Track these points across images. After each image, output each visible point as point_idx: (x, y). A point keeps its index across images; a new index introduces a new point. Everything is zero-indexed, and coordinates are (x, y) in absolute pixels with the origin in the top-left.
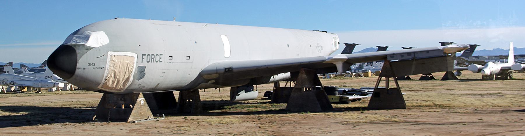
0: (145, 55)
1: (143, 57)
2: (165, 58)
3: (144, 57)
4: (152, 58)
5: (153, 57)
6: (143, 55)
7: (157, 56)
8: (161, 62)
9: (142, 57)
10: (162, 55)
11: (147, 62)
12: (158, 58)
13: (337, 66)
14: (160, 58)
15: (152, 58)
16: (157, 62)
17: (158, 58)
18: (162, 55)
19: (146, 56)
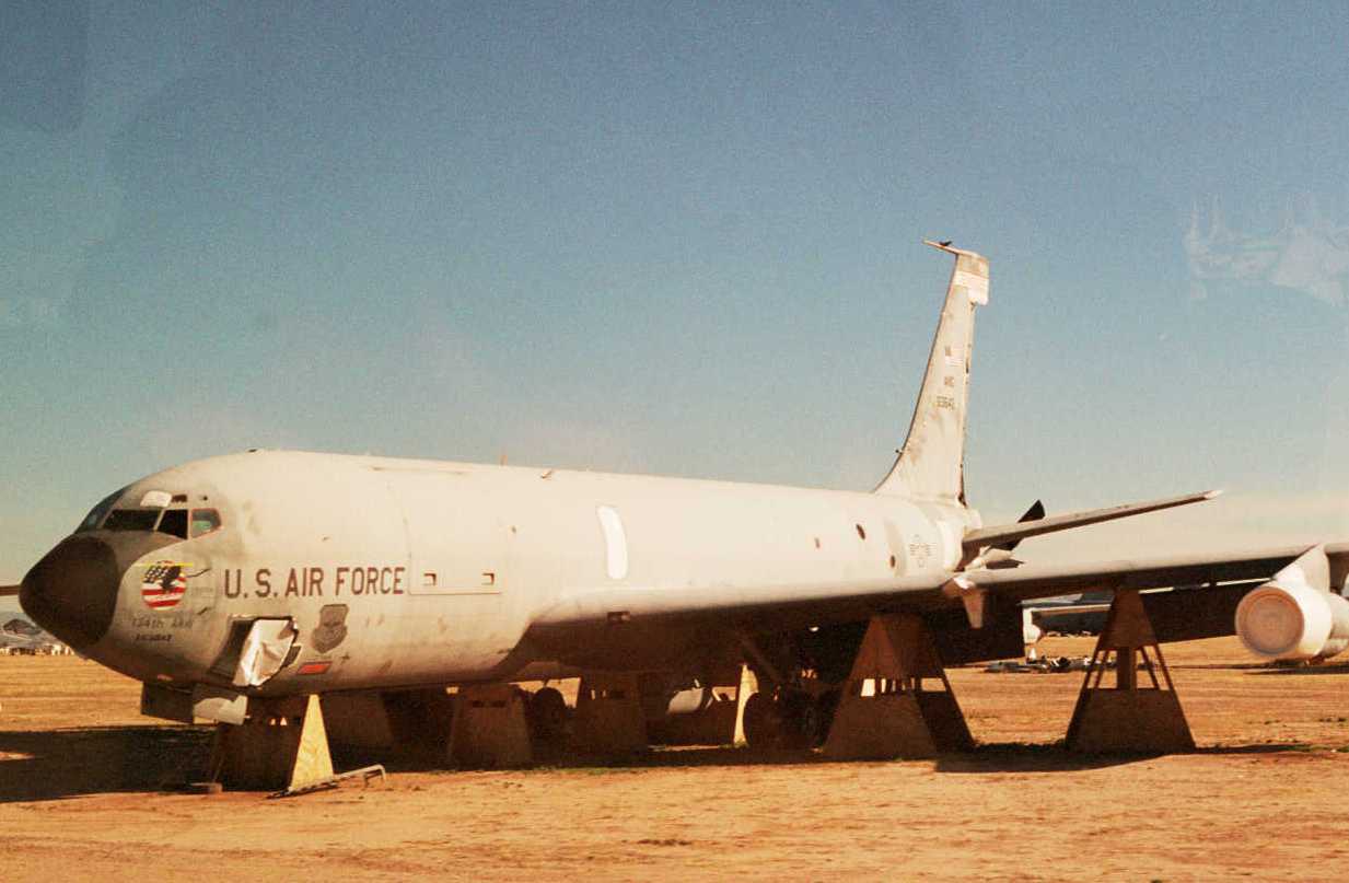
0: (346, 570)
1: (341, 578)
2: (414, 580)
3: (343, 575)
4: (370, 581)
5: (373, 575)
7: (386, 573)
8: (400, 592)
9: (338, 576)
10: (402, 569)
11: (352, 595)
12: (389, 580)
13: (967, 602)
14: (397, 581)
15: (370, 581)
16: (385, 592)
17: (389, 580)
18: (402, 569)
19: (350, 574)
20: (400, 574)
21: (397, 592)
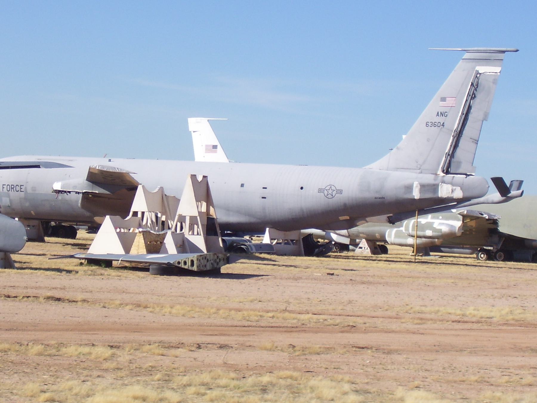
0: (5, 185)
3: (4, 186)
6: (3, 185)
7: (17, 186)
10: (23, 186)
18: (23, 186)
20: (22, 187)
21: (21, 191)
